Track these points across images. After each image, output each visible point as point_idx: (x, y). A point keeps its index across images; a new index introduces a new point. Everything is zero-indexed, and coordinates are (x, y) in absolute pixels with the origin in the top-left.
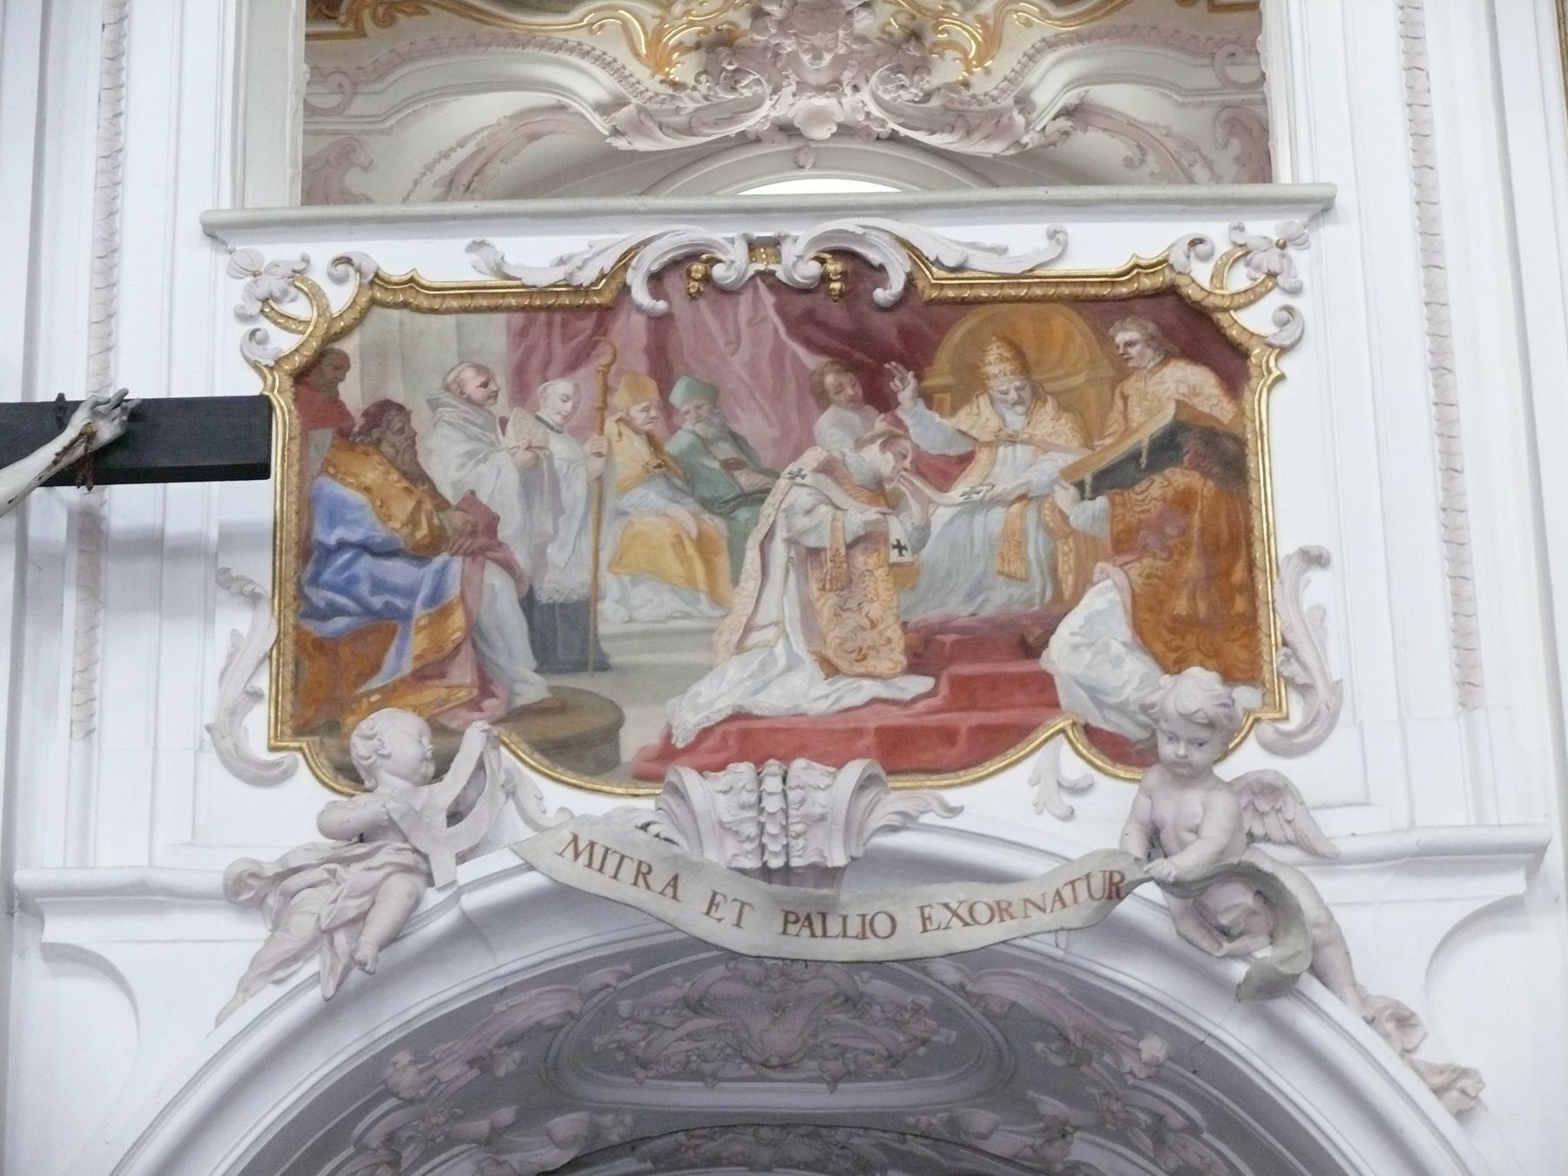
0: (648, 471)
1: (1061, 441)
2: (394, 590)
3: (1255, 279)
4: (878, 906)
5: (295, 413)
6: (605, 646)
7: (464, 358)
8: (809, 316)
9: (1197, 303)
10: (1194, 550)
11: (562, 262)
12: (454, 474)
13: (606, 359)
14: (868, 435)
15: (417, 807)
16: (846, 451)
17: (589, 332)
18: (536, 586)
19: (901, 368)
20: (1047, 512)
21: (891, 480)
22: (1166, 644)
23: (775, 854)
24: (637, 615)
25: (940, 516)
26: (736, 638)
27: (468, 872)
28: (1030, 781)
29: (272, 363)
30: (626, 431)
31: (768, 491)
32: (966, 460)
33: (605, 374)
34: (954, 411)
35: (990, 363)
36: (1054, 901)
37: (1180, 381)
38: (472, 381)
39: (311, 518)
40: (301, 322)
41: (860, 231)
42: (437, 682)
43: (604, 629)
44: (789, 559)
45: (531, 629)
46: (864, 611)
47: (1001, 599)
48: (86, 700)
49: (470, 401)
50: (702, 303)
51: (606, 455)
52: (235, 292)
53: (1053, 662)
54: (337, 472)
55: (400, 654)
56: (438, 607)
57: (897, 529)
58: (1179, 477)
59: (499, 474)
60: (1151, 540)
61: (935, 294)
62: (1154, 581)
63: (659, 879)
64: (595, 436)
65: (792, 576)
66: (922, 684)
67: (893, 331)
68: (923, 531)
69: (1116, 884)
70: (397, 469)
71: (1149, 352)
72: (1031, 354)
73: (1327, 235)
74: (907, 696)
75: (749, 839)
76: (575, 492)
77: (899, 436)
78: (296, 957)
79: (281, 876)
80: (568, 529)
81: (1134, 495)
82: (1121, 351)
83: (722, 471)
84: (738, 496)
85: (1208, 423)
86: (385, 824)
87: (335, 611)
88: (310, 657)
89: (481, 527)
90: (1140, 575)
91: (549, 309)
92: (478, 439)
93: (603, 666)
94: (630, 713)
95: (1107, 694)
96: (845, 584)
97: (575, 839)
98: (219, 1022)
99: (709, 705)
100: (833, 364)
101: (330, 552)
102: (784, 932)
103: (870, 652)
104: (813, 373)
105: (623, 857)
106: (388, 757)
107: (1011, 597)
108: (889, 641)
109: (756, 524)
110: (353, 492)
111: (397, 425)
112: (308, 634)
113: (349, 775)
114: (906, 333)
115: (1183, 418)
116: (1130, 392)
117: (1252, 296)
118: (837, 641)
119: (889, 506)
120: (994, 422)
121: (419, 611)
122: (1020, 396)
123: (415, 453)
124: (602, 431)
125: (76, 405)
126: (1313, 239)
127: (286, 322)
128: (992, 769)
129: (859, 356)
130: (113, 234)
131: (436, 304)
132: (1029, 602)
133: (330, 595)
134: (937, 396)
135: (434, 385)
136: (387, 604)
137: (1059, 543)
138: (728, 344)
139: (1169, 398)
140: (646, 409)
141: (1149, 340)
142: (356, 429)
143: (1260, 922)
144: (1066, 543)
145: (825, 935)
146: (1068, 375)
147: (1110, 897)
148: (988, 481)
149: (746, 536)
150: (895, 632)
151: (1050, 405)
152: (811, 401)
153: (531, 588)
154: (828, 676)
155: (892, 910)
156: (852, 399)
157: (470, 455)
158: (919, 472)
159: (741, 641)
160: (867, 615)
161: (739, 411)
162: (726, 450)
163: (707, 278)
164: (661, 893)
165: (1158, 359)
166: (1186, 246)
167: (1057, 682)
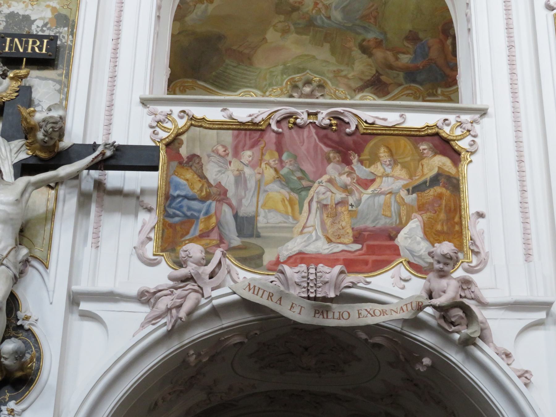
0: (274, 179)
1: (402, 177)
2: (195, 210)
3: (463, 132)
4: (344, 310)
5: (166, 156)
6: (259, 230)
7: (218, 143)
8: (326, 136)
9: (446, 138)
10: (443, 211)
11: (250, 116)
12: (215, 177)
13: (262, 146)
14: (343, 172)
15: (200, 272)
16: (336, 176)
17: (258, 137)
18: (238, 211)
19: (353, 153)
20: (398, 198)
21: (349, 185)
22: (434, 238)
23: (312, 293)
24: (269, 221)
25: (365, 197)
26: (300, 230)
27: (215, 294)
28: (391, 277)
29: (159, 140)
30: (268, 167)
31: (311, 187)
32: (373, 181)
33: (262, 150)
34: (369, 167)
35: (381, 153)
36: (400, 310)
37: (439, 161)
38: (221, 150)
39: (169, 187)
40: (169, 129)
41: (342, 111)
42: (206, 238)
43: (259, 225)
44: (317, 208)
45: (236, 224)
46: (340, 224)
47: (382, 222)
48: (97, 237)
49: (220, 155)
50: (293, 131)
51: (262, 174)
52: (150, 120)
53: (399, 242)
54: (178, 174)
55: (195, 229)
56: (208, 216)
57: (351, 200)
58: (439, 189)
59: (228, 177)
60: (430, 208)
61: (365, 131)
62: (430, 220)
63: (275, 298)
64: (258, 168)
65: (318, 212)
66: (357, 246)
67: (352, 142)
68: (359, 201)
69: (420, 306)
70: (197, 174)
71: (430, 152)
72: (394, 151)
73: (485, 120)
74: (353, 250)
75: (304, 288)
76: (252, 184)
77: (352, 173)
78: (160, 317)
79: (155, 293)
80: (250, 194)
81: (425, 194)
82: (421, 151)
83: (298, 180)
84: (302, 188)
85: (448, 174)
86: (190, 277)
87: (175, 215)
88: (167, 229)
89: (222, 193)
90: (426, 218)
91: (246, 130)
92: (222, 167)
93: (258, 236)
94: (266, 251)
95: (415, 253)
96: (335, 216)
97: (249, 285)
98: (133, 336)
99: (291, 250)
100: (333, 150)
101: (174, 198)
102: (315, 316)
103: (342, 236)
104: (326, 153)
105: (264, 291)
106: (191, 257)
107: (386, 222)
108: (348, 233)
109: (308, 196)
110: (182, 180)
111: (197, 161)
112: (167, 222)
114: (355, 142)
115: (440, 172)
116: (424, 163)
117: (462, 137)
118: (331, 232)
119: (349, 193)
120: (382, 170)
121: (202, 217)
122: (390, 163)
123: (202, 170)
124: (260, 167)
125: (99, 145)
126: (481, 121)
127: (165, 129)
128: (379, 272)
129: (341, 148)
131: (211, 126)
132: (392, 223)
133: (174, 211)
134: (364, 162)
135: (209, 150)
136: (192, 214)
137: (401, 207)
138: (300, 143)
139: (436, 166)
140: (274, 161)
141: (430, 149)
142: (185, 162)
143: (465, 321)
144: (404, 207)
145: (327, 318)
146: (404, 158)
147: (418, 310)
148: (379, 187)
149: (304, 200)
150: (350, 231)
151: (399, 167)
152: (325, 161)
153: (237, 212)
154: (328, 243)
155: (349, 311)
156: (338, 161)
157: (219, 171)
158: (359, 184)
159: (302, 230)
160: (341, 225)
161: (303, 163)
162: (299, 174)
163: (295, 124)
164: (276, 303)
165: (433, 154)
166: (442, 121)
167: (400, 248)
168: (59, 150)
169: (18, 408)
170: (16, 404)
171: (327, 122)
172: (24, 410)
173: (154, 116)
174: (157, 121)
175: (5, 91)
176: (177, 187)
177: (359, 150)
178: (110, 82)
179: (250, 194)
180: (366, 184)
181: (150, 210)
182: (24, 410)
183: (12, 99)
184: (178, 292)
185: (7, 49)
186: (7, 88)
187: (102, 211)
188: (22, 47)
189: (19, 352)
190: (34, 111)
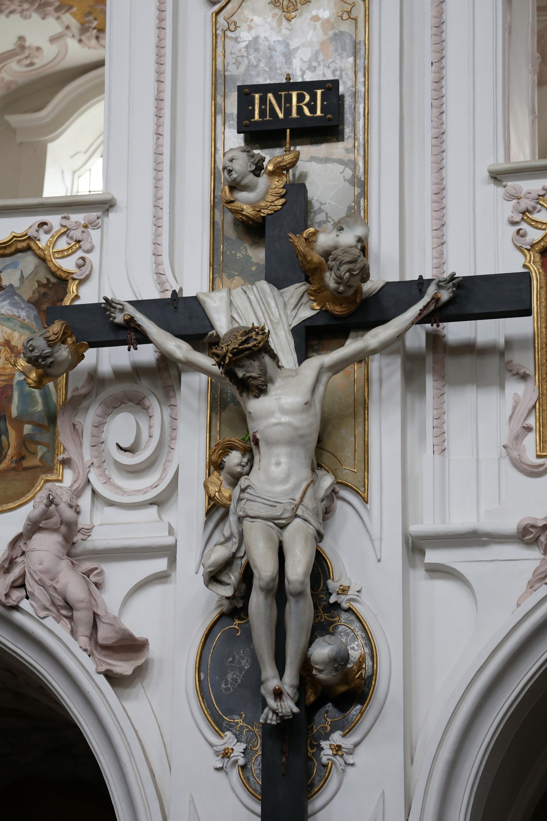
5: (543, 273)
29: (529, 247)
98: (518, 605)
125: (430, 281)
130: (442, 180)
168: (364, 297)
169: (347, 743)
170: (344, 736)
172: (356, 745)
173: (515, 201)
174: (521, 212)
175: (263, 199)
178: (435, 146)
181: (524, 377)
182: (356, 745)
183: (275, 211)
185: (257, 117)
186: (266, 193)
187: (444, 386)
188: (281, 109)
189: (339, 660)
190: (315, 233)
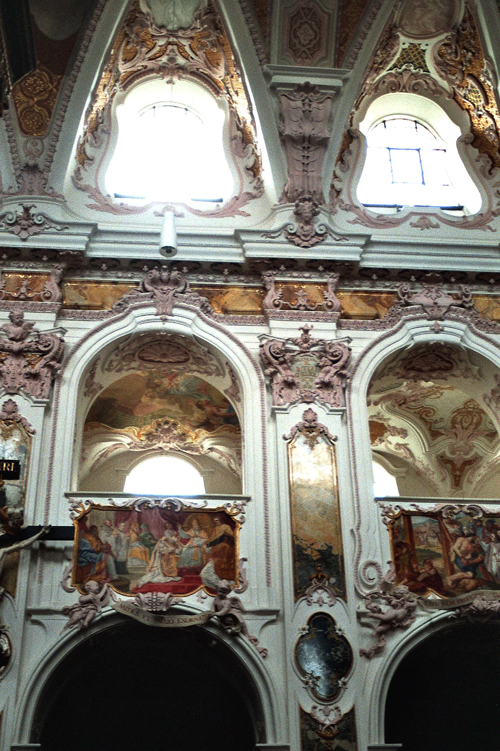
27: (103, 610)
34: (187, 531)
47: (193, 564)
48: (41, 577)
57: (177, 551)
58: (223, 544)
63: (135, 612)
66: (179, 578)
68: (181, 552)
73: (249, 504)
76: (124, 543)
79: (72, 609)
93: (127, 573)
94: (132, 581)
96: (168, 561)
113: (85, 591)
117: (236, 514)
121: (97, 563)
125: (42, 527)
141: (220, 520)
162: (150, 536)
163: (148, 507)
171: (165, 505)
176: (84, 545)
177: (182, 521)
179: (123, 548)
180: (185, 541)
181: (69, 560)
184: (84, 609)
190: (7, 508)
